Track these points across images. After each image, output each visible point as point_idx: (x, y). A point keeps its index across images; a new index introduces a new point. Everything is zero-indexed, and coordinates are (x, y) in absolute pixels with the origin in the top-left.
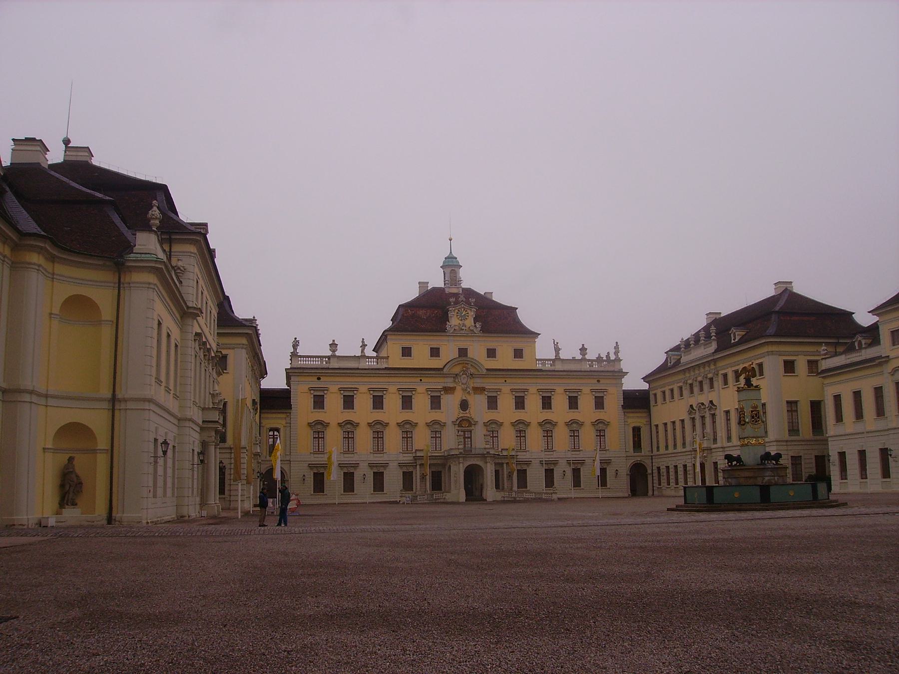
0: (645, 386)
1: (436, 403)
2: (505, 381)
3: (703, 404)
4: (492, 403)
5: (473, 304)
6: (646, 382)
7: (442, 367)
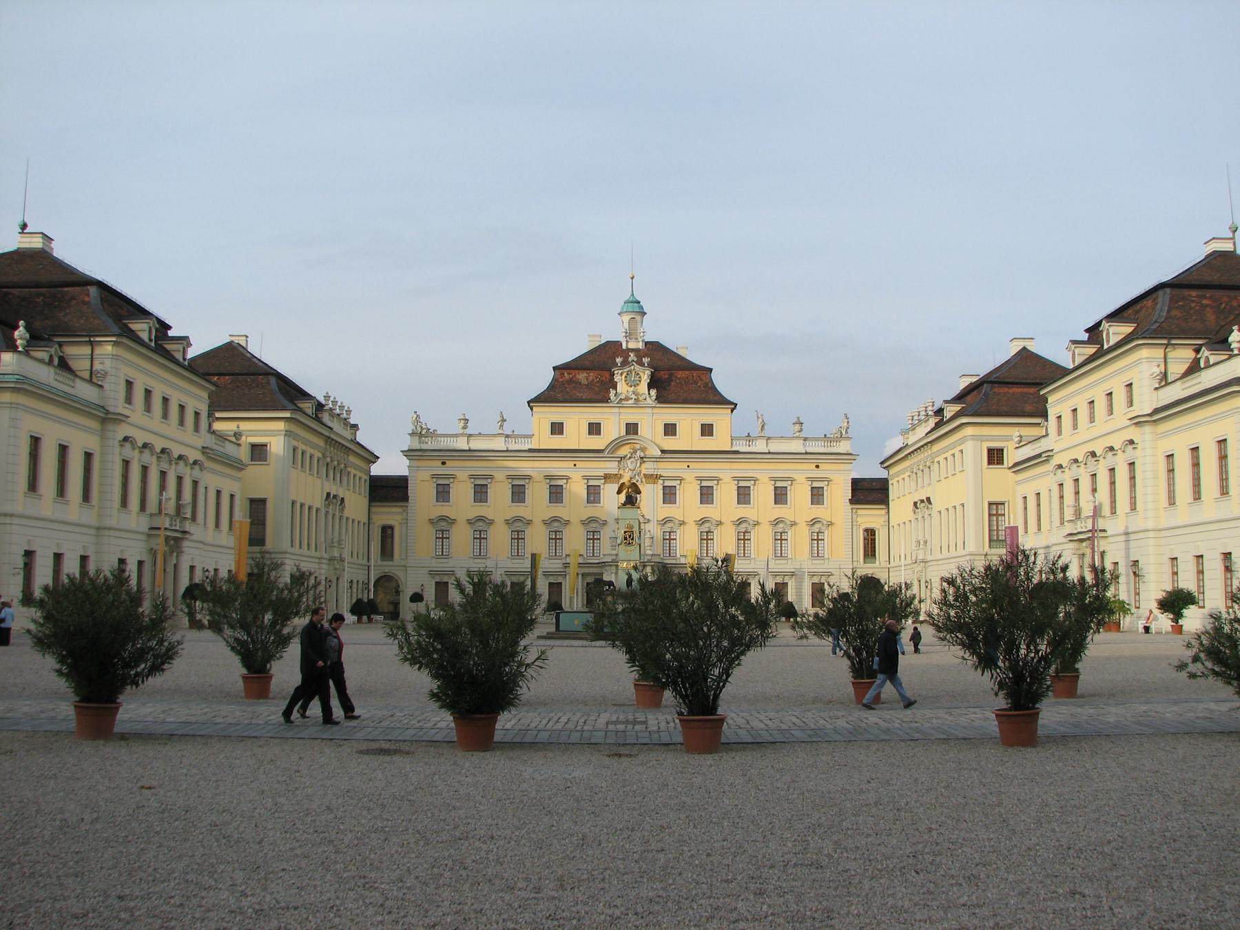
2: (688, 466)
3: (922, 501)
4: (669, 495)
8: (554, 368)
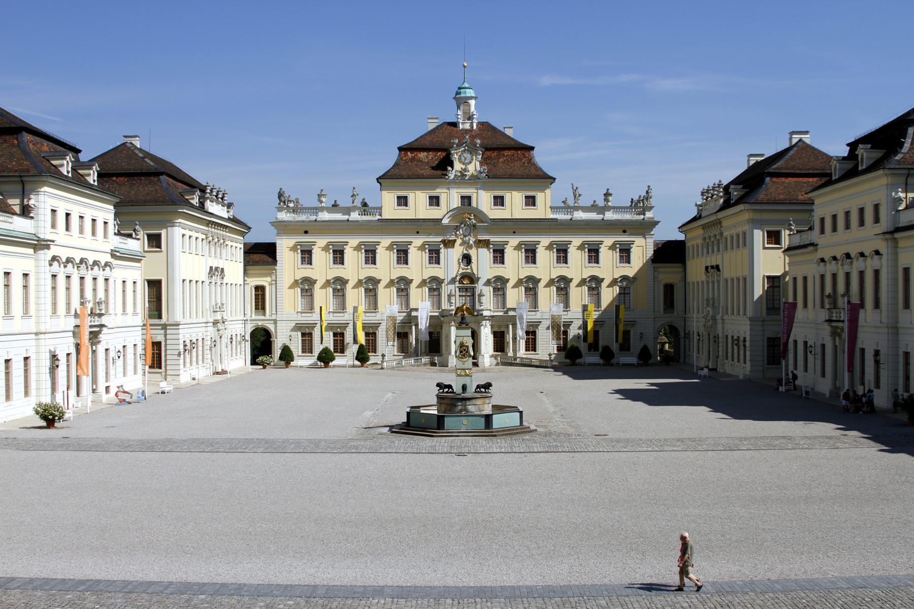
0: (681, 237)
1: (435, 256)
4: (499, 255)
5: (478, 146)
6: (681, 232)
7: (441, 218)
8: (400, 149)
